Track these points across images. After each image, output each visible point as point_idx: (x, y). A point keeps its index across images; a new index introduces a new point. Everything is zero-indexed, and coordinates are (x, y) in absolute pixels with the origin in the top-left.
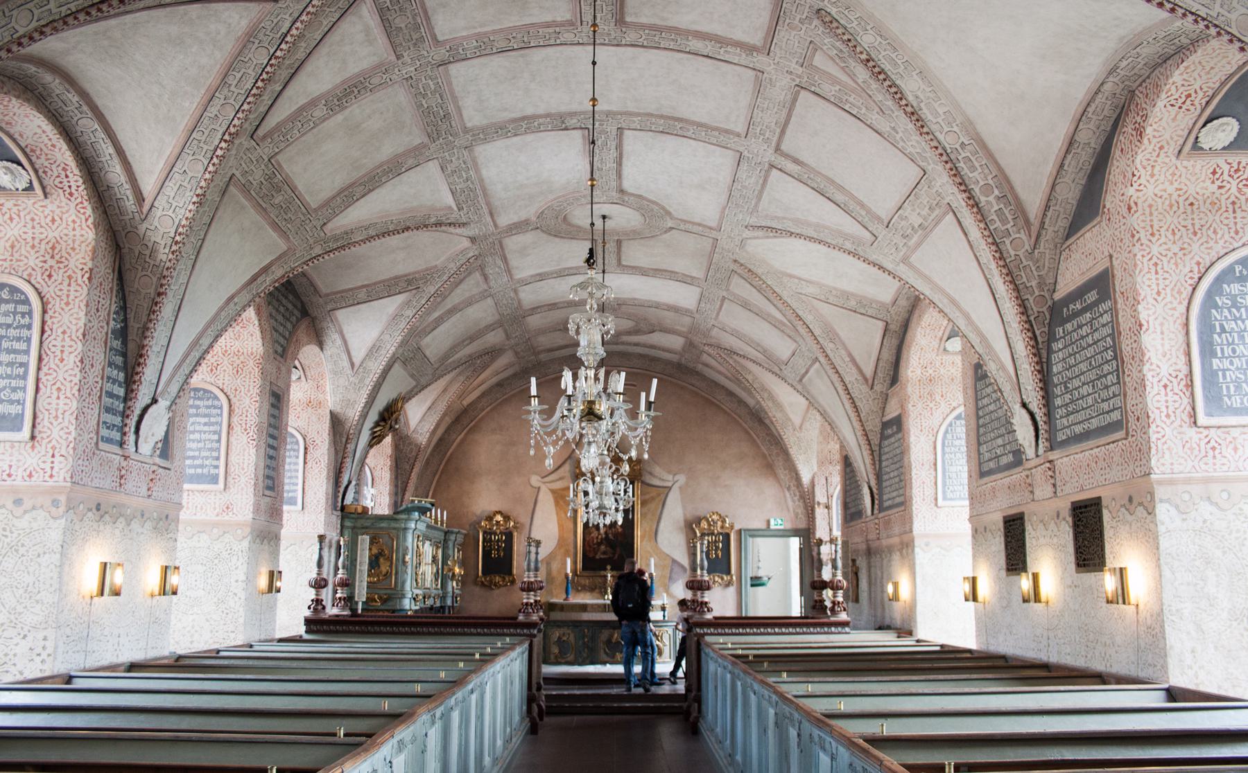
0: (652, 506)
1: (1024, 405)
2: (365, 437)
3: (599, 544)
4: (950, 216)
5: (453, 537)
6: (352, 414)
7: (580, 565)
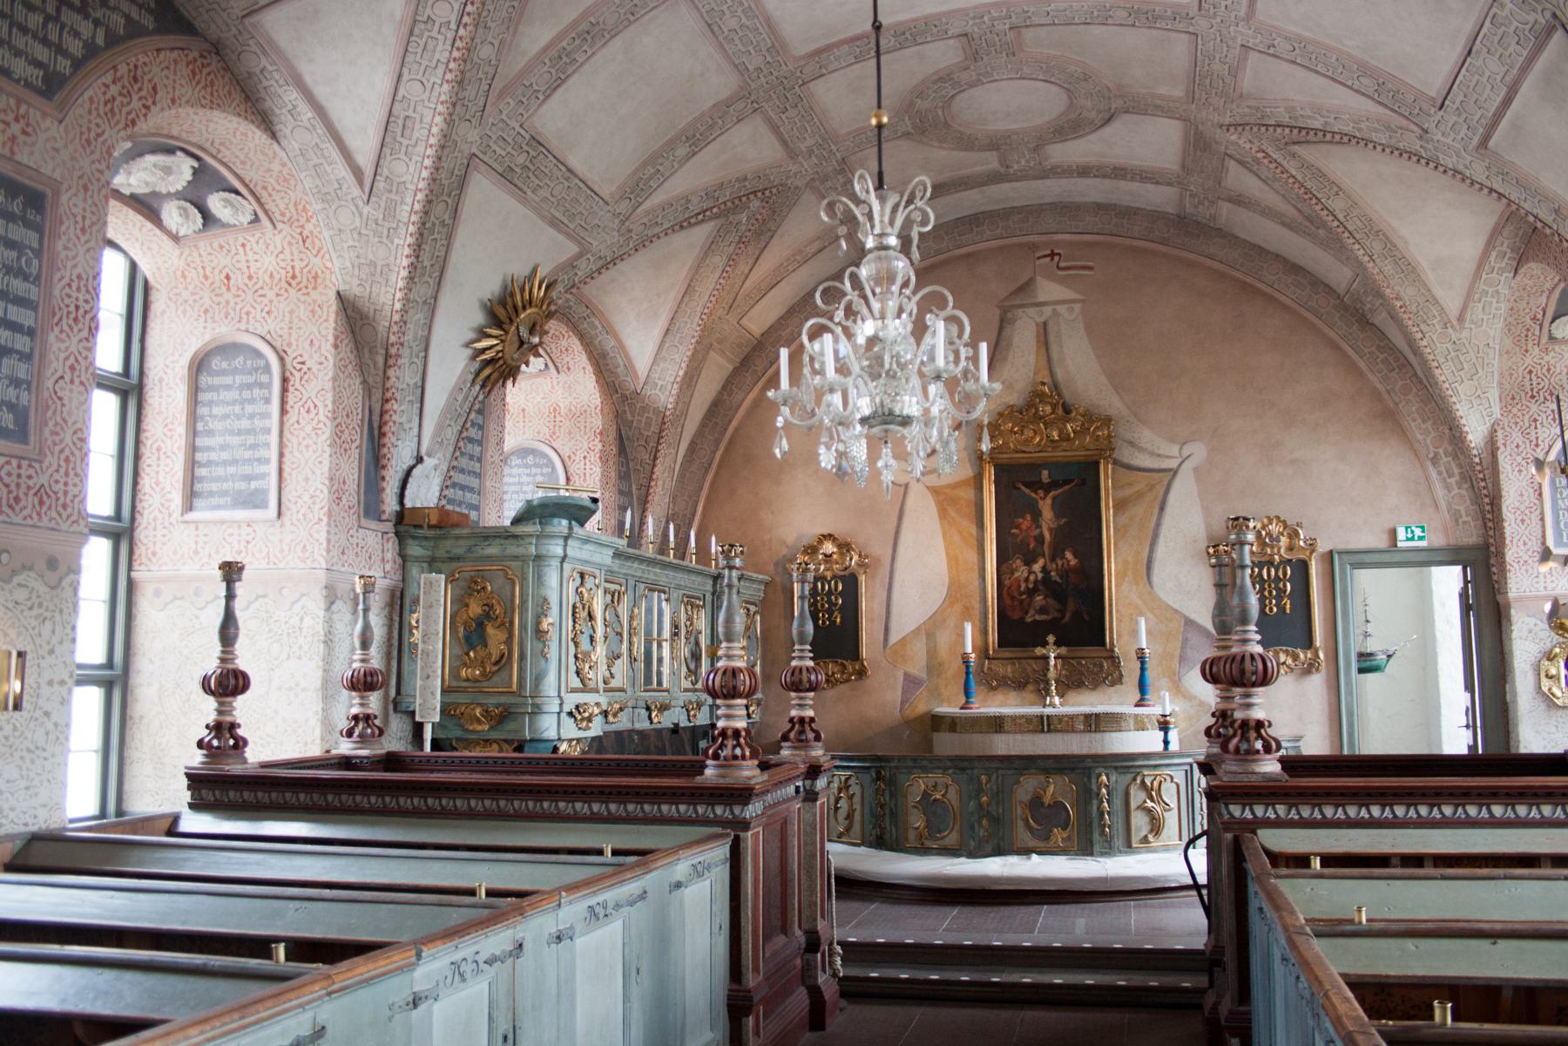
0: (1138, 510)
3: (1032, 592)
7: (993, 637)
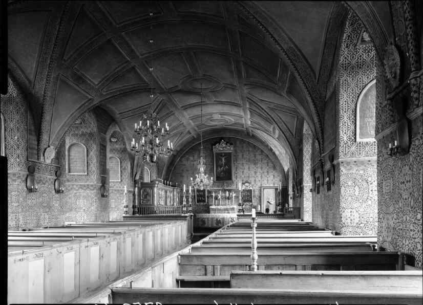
1: (317, 139)
5: (175, 190)
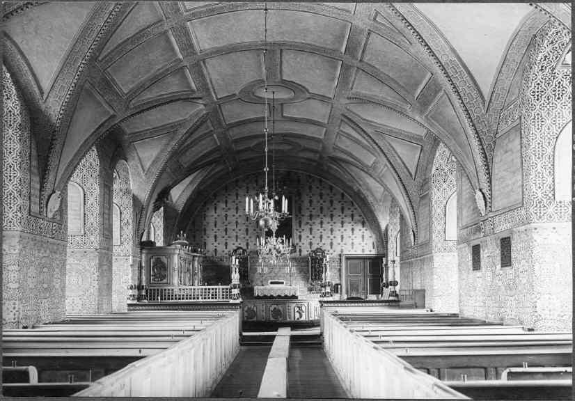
1: (480, 190)
2: (151, 207)
4: (446, 96)
5: (197, 259)
6: (143, 196)
